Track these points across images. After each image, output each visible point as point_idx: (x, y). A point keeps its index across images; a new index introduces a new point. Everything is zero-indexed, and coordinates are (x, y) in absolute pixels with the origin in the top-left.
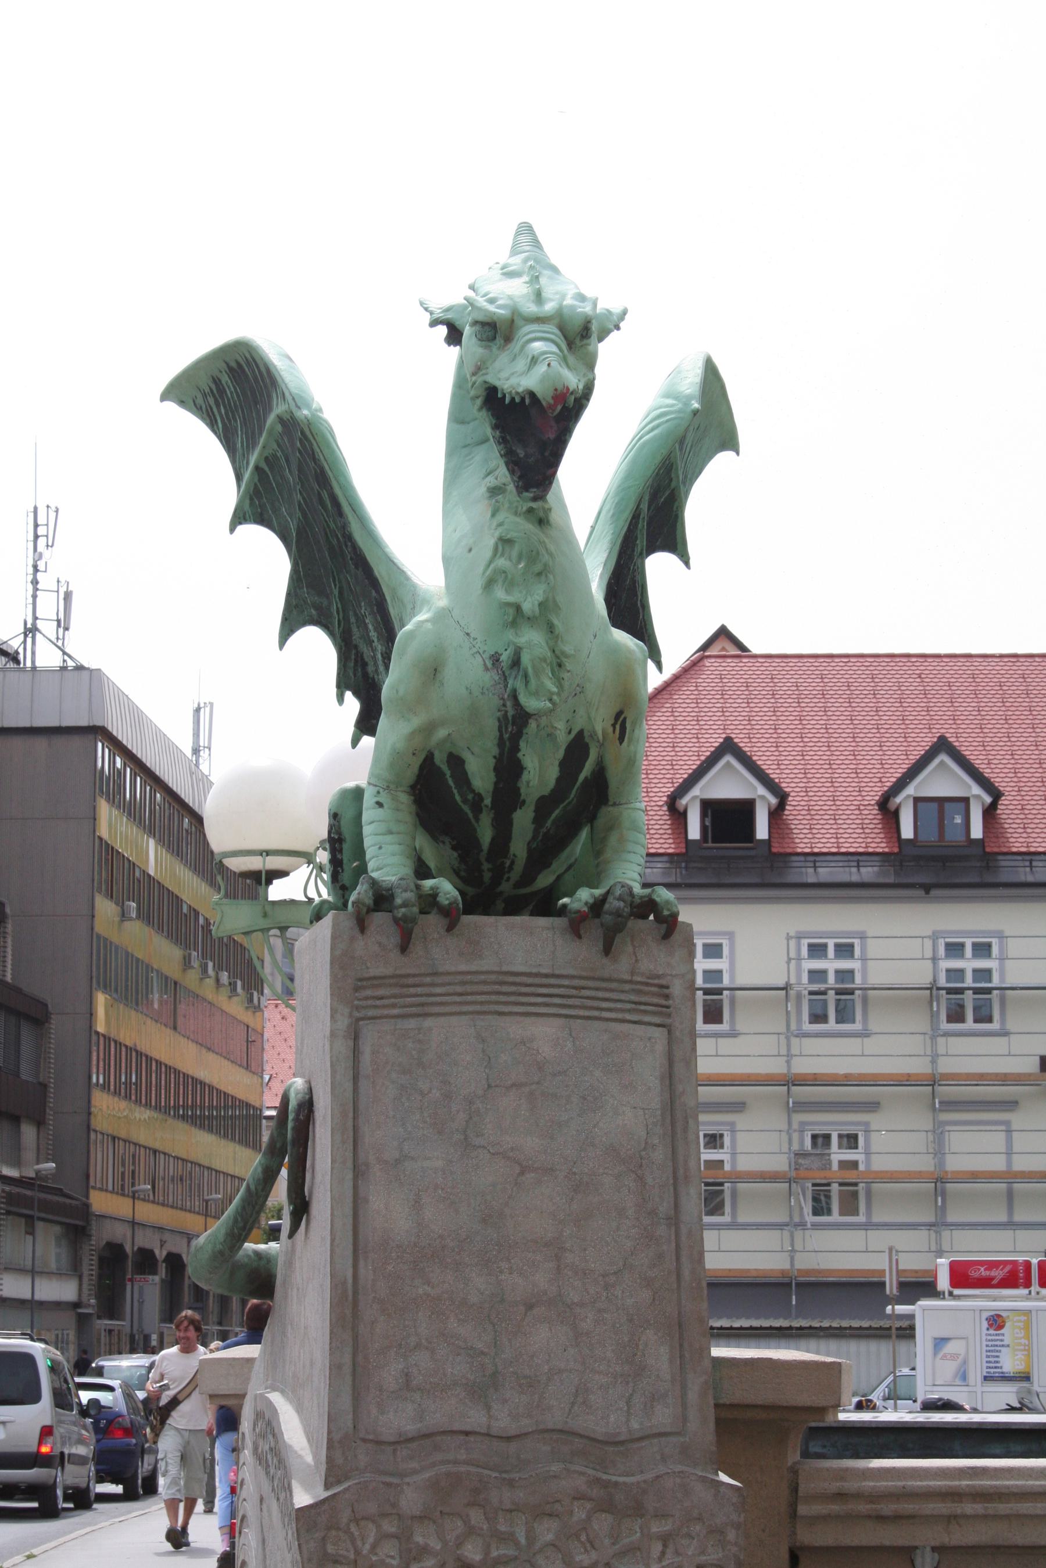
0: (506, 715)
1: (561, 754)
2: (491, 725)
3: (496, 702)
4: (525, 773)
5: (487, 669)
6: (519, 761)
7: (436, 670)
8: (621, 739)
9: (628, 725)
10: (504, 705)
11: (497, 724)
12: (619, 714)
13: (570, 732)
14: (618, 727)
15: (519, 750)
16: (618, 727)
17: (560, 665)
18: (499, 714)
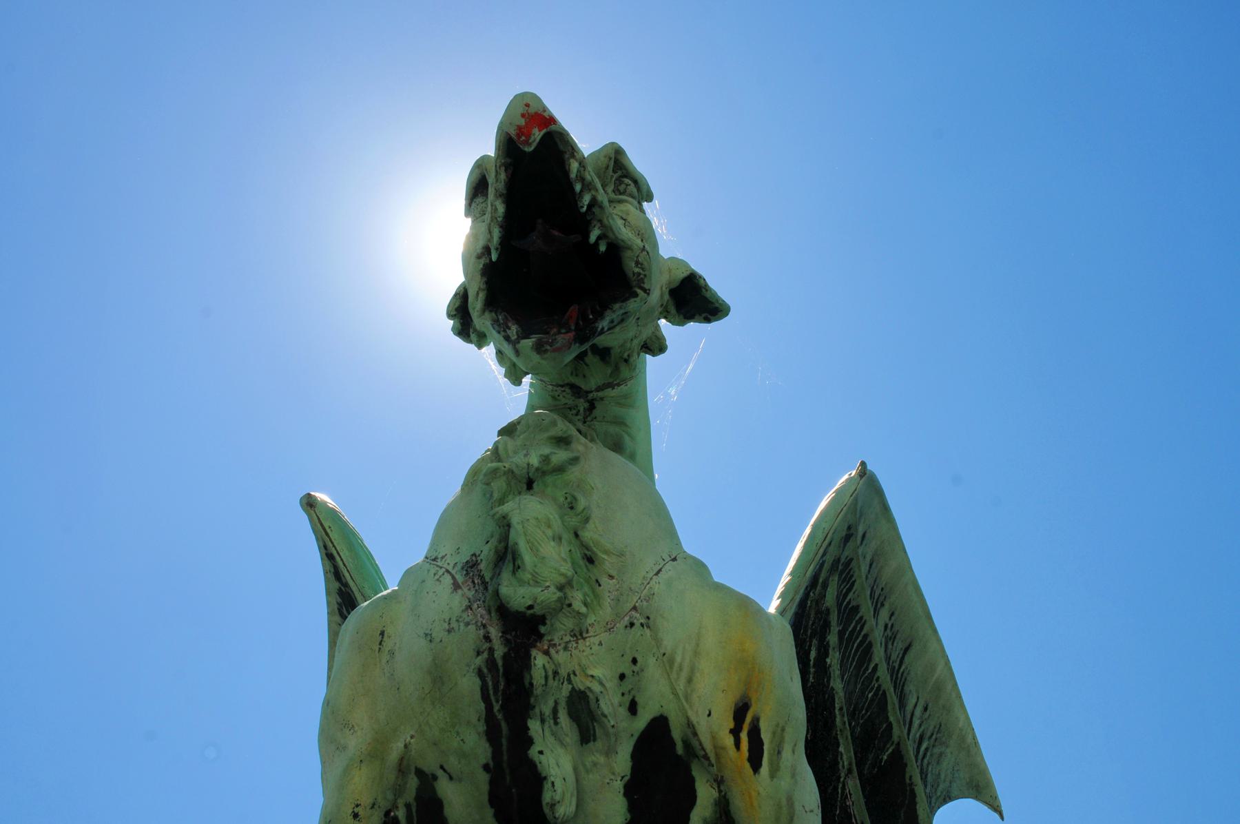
0: (491, 662)
1: (622, 762)
2: (468, 685)
3: (472, 635)
4: (547, 786)
5: (456, 586)
6: (532, 766)
7: (382, 633)
8: (755, 761)
9: (766, 736)
10: (487, 638)
11: (478, 681)
12: (741, 711)
13: (633, 708)
14: (744, 736)
15: (530, 742)
16: (744, 736)
17: (590, 560)
18: (479, 661)
